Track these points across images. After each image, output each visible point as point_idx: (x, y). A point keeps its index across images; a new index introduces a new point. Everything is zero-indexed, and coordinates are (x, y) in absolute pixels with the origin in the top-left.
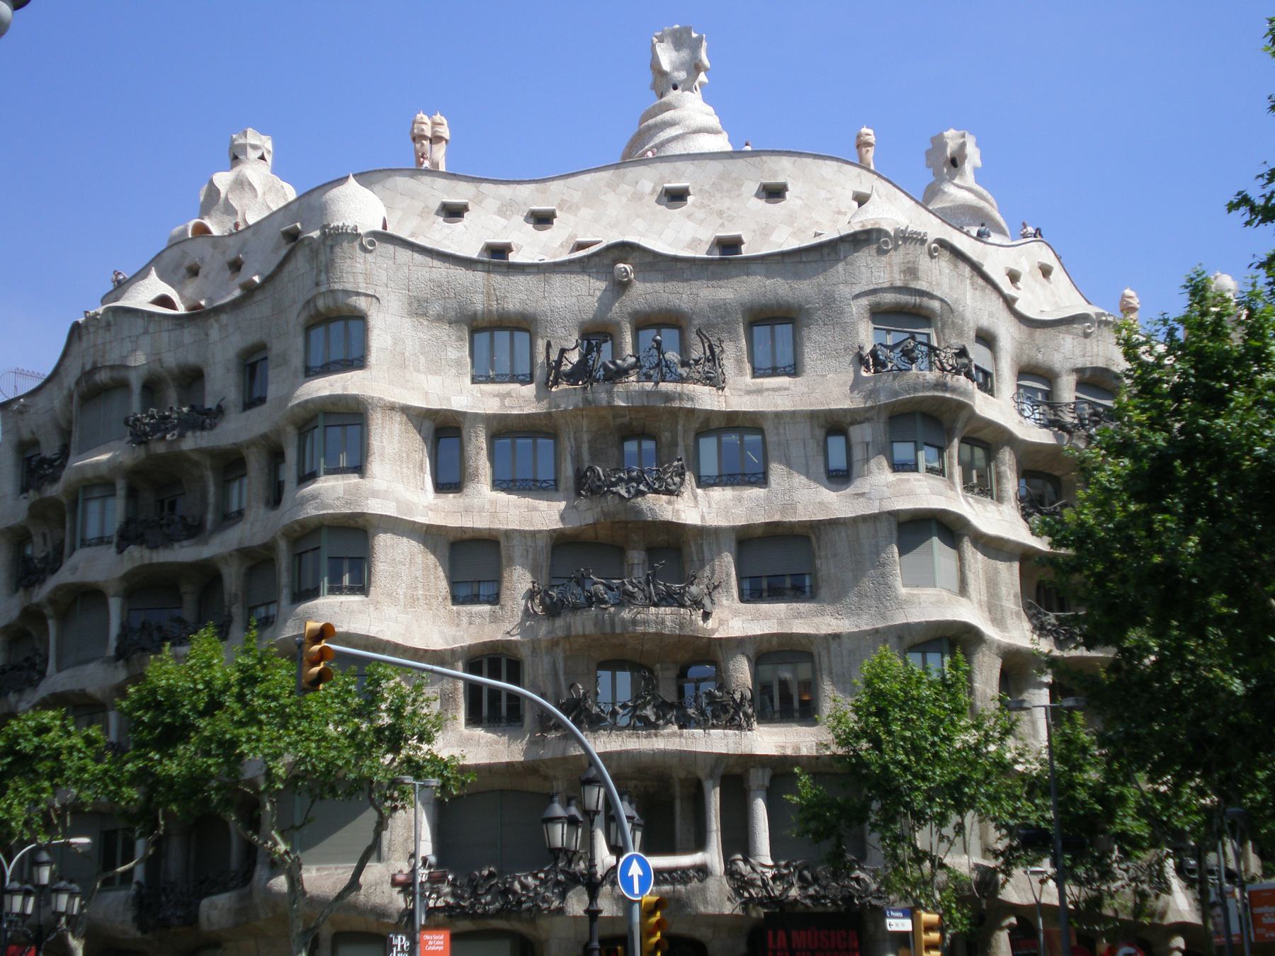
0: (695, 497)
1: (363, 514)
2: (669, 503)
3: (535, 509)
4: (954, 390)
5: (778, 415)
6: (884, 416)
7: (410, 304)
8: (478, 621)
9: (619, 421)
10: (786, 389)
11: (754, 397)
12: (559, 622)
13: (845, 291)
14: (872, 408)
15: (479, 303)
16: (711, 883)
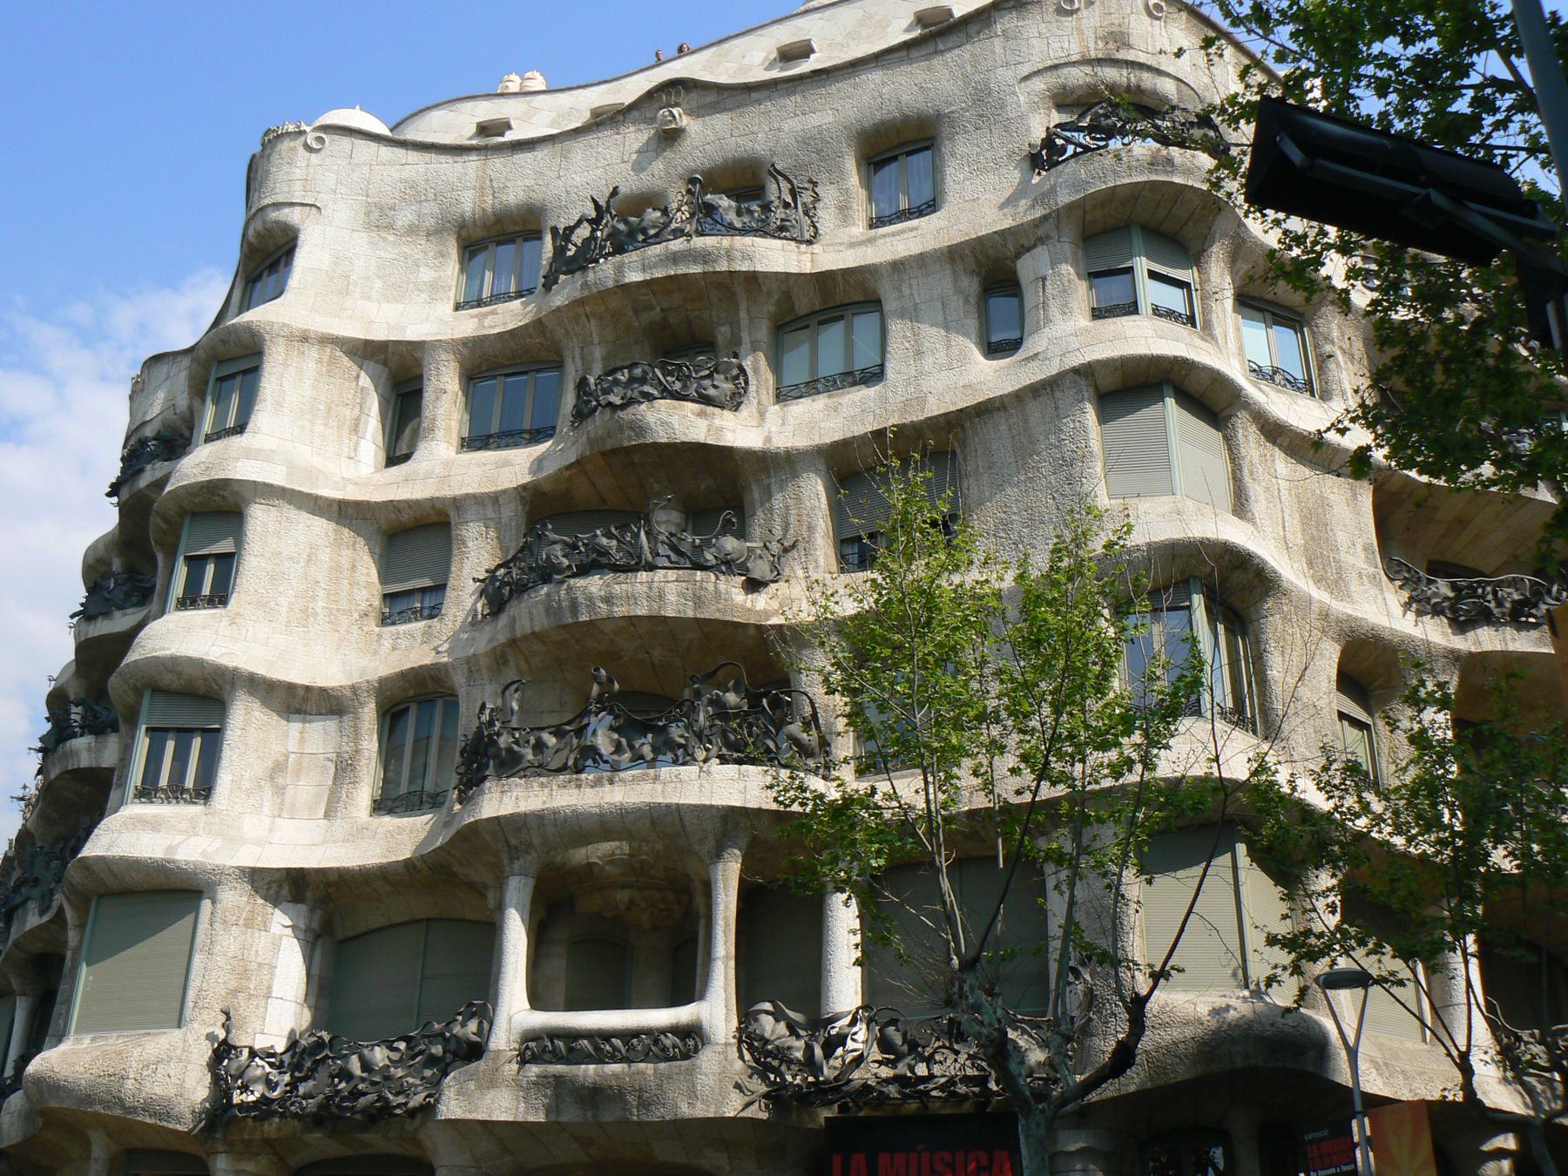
0: (762, 414)
1: (226, 483)
2: (701, 414)
3: (507, 463)
4: (1188, 172)
5: (898, 266)
6: (1069, 233)
7: (368, 214)
8: (403, 643)
9: (647, 317)
10: (912, 230)
11: (860, 251)
12: (504, 619)
13: (1005, 76)
14: (1045, 218)
15: (468, 203)
16: (708, 1061)
